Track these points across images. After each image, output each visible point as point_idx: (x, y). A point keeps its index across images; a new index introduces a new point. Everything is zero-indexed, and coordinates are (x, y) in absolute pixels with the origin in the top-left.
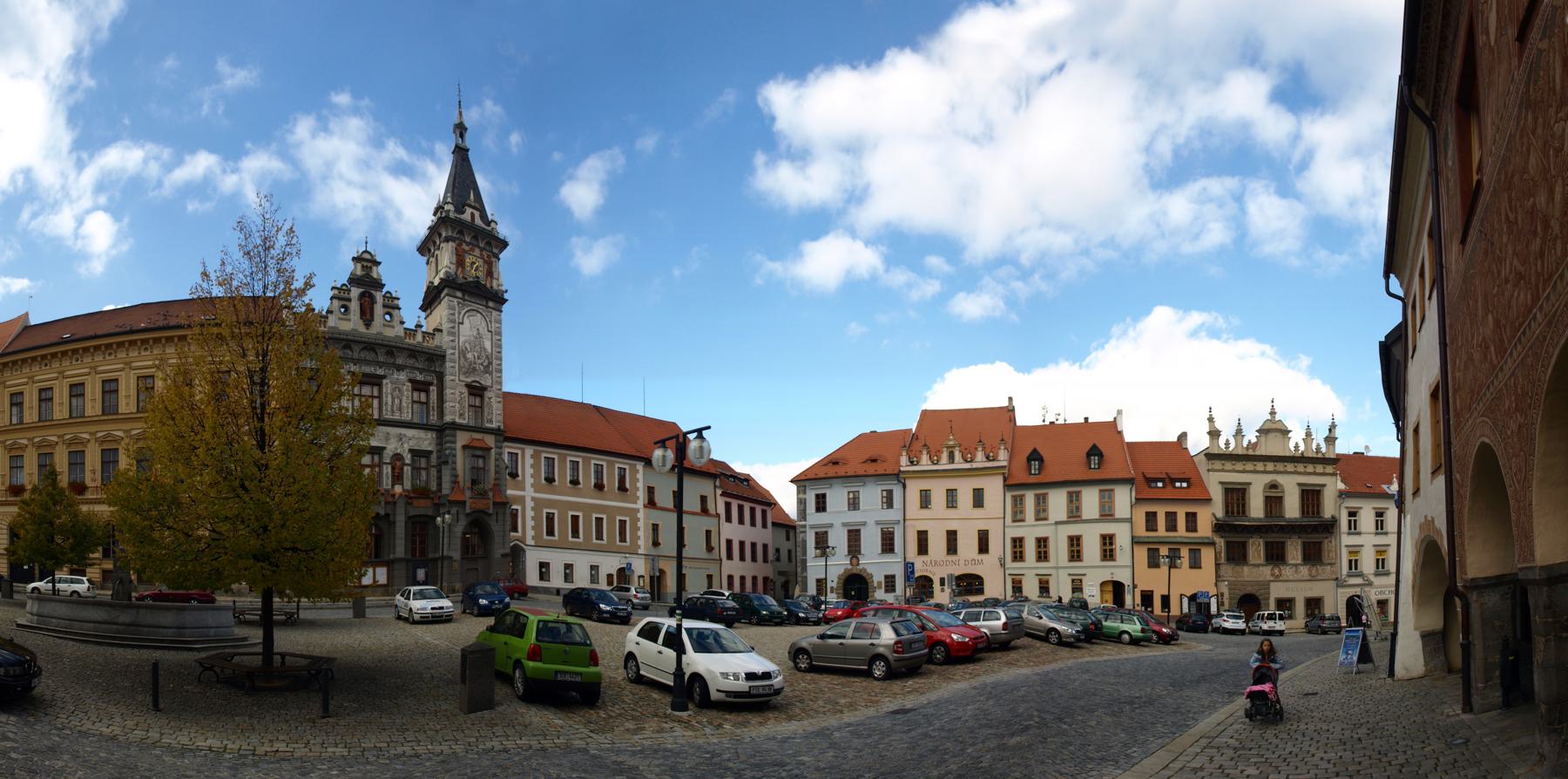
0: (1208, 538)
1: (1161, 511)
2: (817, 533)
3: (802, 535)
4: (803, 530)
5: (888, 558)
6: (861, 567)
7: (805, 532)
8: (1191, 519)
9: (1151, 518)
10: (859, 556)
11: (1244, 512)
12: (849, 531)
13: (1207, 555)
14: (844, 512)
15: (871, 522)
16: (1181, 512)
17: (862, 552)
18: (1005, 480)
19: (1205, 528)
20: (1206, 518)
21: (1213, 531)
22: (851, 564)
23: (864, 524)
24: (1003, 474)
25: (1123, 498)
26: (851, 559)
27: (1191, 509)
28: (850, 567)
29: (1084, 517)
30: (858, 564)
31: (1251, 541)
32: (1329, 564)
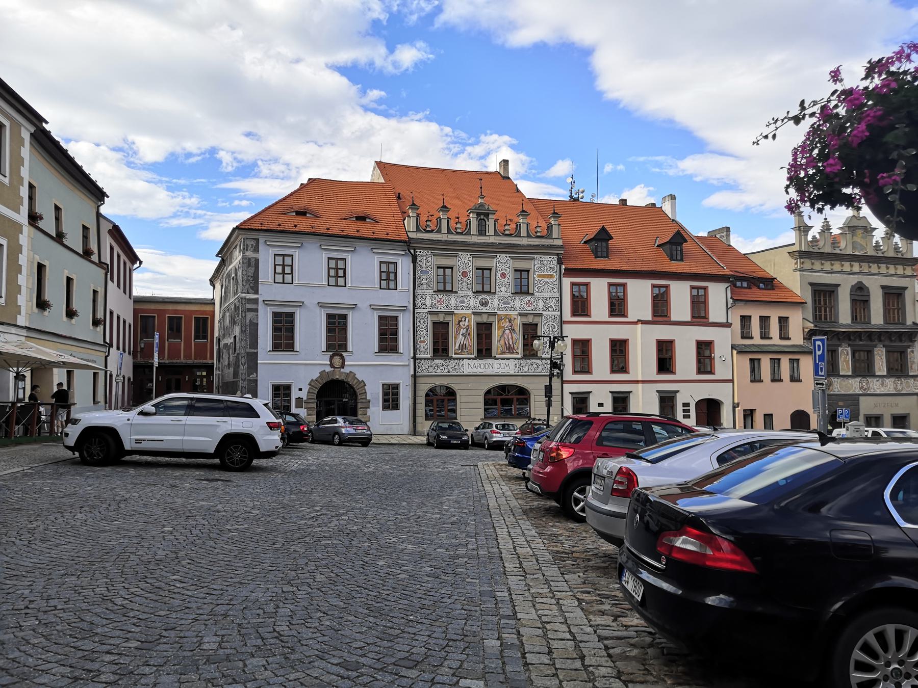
0: (801, 346)
1: (755, 314)
2: (275, 315)
3: (250, 315)
4: (254, 307)
5: (388, 359)
6: (346, 370)
7: (256, 310)
8: (783, 321)
9: (745, 320)
10: (344, 354)
11: (831, 318)
12: (329, 316)
13: (807, 365)
14: (321, 287)
15: (363, 305)
16: (775, 315)
17: (350, 348)
18: (560, 262)
19: (797, 338)
20: (799, 323)
21: (804, 339)
22: (332, 365)
23: (354, 307)
24: (557, 254)
25: (717, 294)
26: (331, 358)
27: (784, 314)
28: (328, 369)
29: (674, 318)
30: (343, 366)
31: (840, 349)
32: (913, 376)
